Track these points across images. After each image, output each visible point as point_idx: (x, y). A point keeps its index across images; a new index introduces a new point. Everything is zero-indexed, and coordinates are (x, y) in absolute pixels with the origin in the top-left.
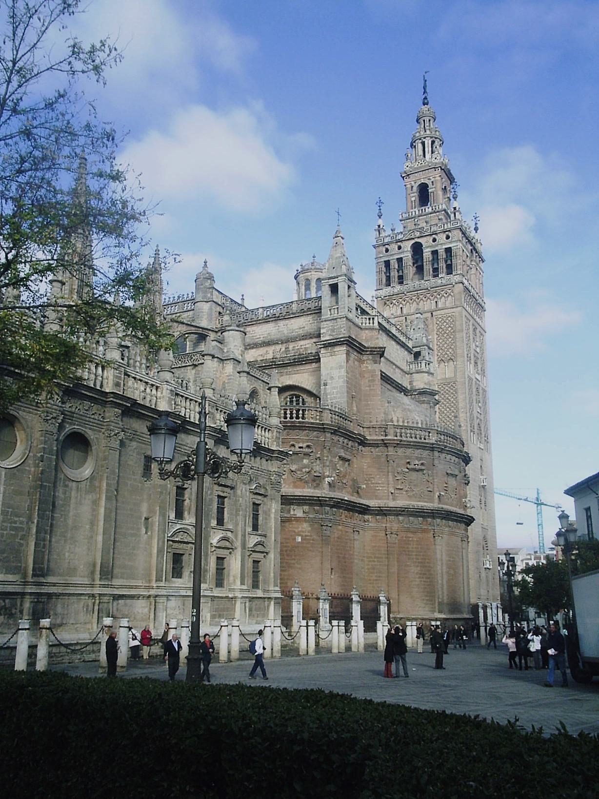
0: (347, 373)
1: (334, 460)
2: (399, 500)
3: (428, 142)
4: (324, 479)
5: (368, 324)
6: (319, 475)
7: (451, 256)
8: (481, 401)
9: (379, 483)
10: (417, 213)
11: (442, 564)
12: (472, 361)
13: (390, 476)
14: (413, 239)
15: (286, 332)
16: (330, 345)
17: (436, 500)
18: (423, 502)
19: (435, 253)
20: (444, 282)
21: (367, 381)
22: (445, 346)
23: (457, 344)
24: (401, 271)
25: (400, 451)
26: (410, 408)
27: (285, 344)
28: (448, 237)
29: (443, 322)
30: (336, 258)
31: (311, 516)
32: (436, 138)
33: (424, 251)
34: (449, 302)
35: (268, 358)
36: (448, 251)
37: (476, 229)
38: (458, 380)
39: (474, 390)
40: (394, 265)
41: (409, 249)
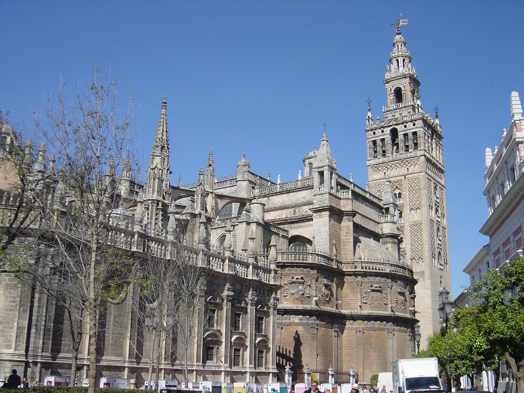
0: (330, 228)
1: (319, 286)
2: (365, 310)
3: (401, 60)
4: (312, 298)
5: (344, 196)
6: (310, 296)
9: (352, 300)
10: (394, 108)
11: (393, 350)
12: (434, 208)
15: (294, 200)
16: (318, 211)
17: (390, 310)
18: (381, 311)
19: (406, 135)
21: (344, 233)
22: (414, 199)
23: (422, 197)
24: (384, 147)
25: (366, 279)
26: (375, 249)
27: (293, 209)
28: (414, 125)
29: (412, 182)
31: (304, 322)
32: (406, 57)
33: (399, 134)
34: (417, 169)
35: (283, 217)
36: (415, 134)
38: (423, 222)
40: (379, 143)
41: (389, 133)
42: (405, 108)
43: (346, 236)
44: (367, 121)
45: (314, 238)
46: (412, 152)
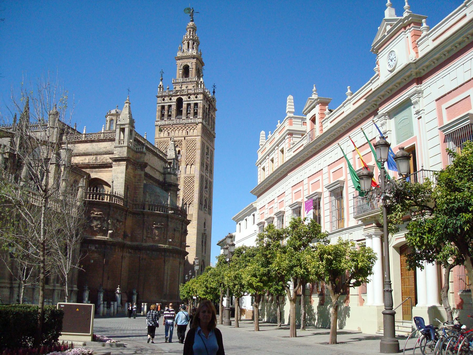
7: (197, 108)
8: (208, 188)
13: (145, 231)
14: (178, 95)
15: (96, 149)
16: (116, 160)
17: (167, 243)
19: (189, 105)
20: (192, 121)
24: (170, 112)
27: (95, 156)
30: (125, 114)
33: (184, 103)
37: (214, 92)
39: (204, 181)
40: (166, 108)
42: (191, 83)
43: (138, 183)
44: (159, 89)
45: (113, 182)
46: (192, 119)
